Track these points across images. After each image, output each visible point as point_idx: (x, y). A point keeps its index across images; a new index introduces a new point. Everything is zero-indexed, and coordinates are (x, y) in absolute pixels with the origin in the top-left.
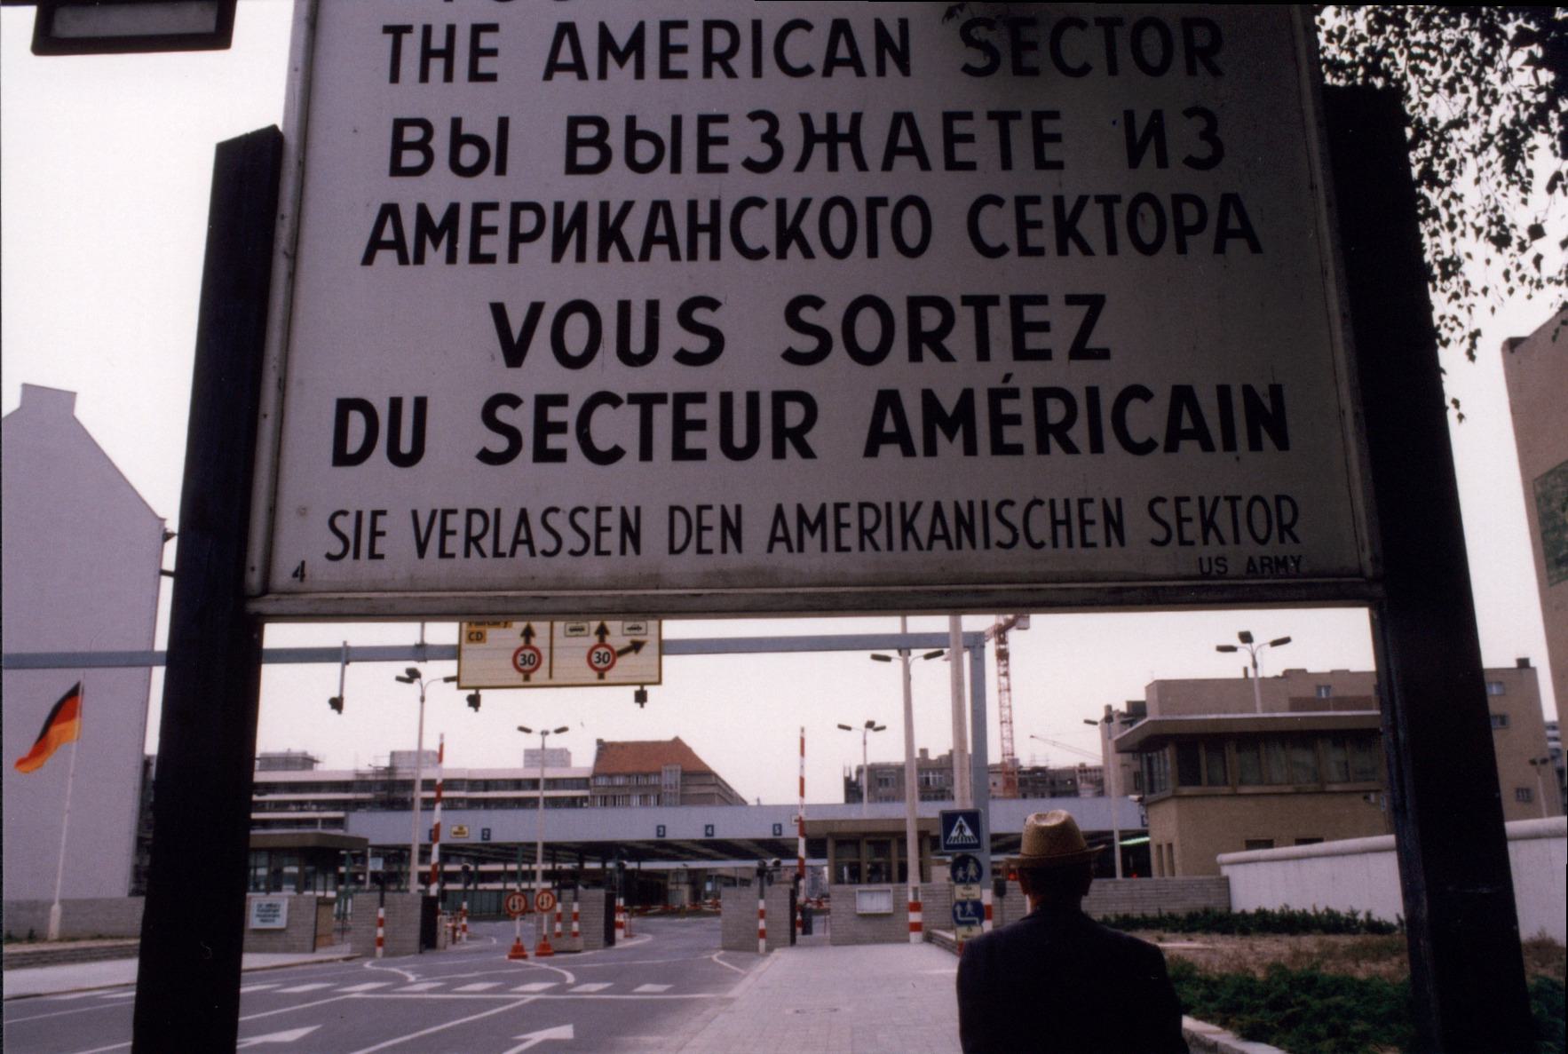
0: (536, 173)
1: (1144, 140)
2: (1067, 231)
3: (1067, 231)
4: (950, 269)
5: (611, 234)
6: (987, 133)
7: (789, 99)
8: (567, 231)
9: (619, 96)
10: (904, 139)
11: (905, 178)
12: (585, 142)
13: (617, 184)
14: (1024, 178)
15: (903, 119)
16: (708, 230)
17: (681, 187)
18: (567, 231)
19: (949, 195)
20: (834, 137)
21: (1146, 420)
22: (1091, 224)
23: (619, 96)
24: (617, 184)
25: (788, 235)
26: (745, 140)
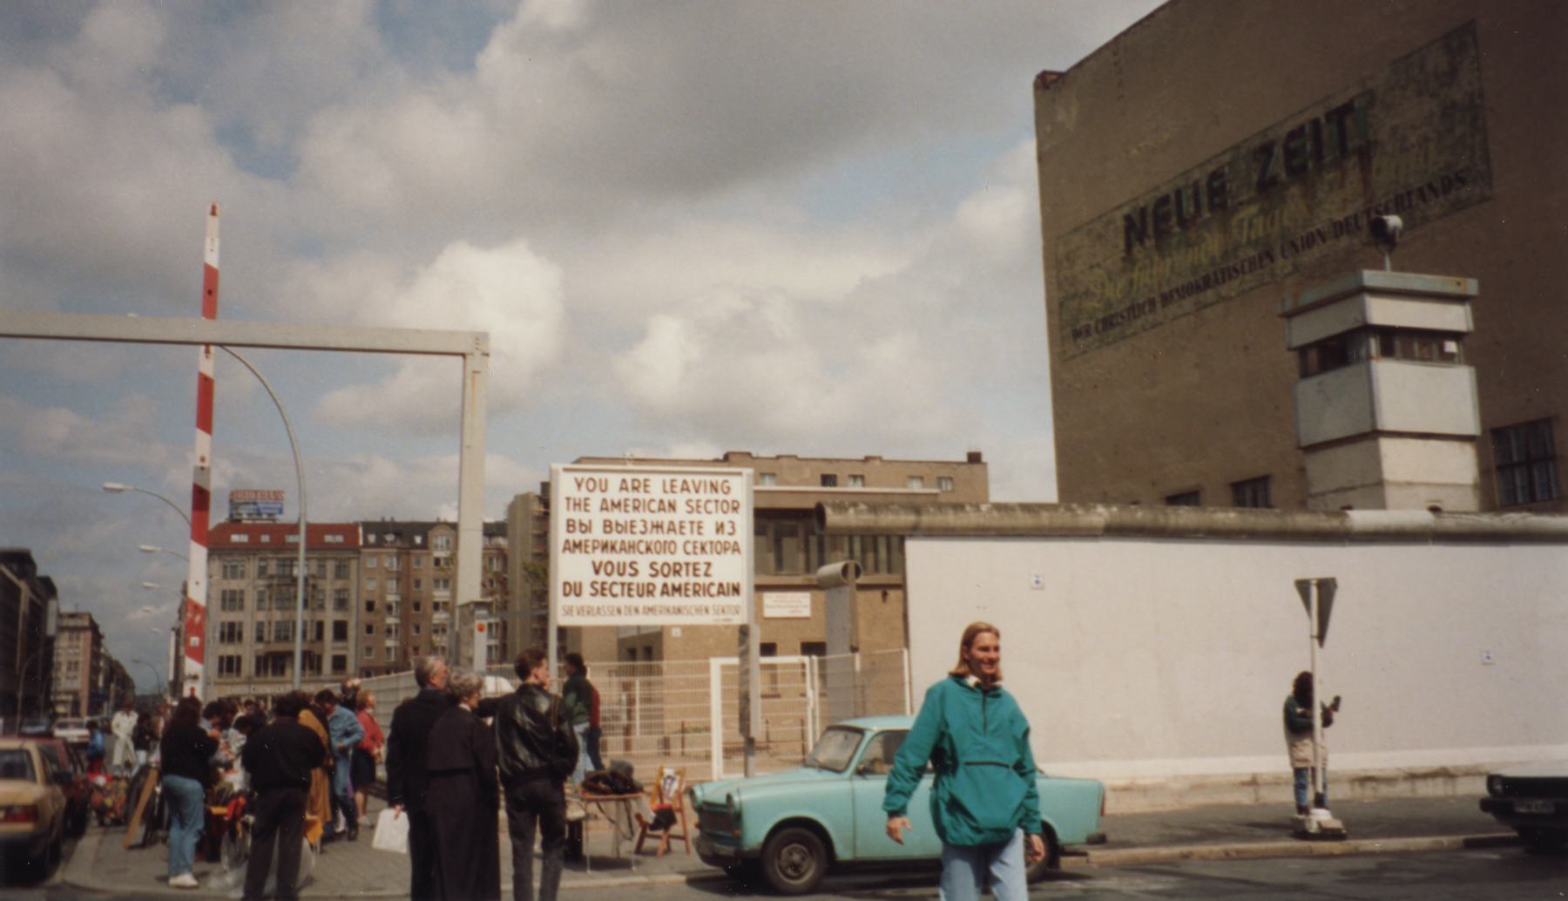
0: (598, 533)
1: (720, 528)
2: (703, 548)
3: (703, 548)
4: (680, 557)
5: (613, 548)
6: (687, 526)
7: (651, 518)
8: (605, 547)
9: (616, 516)
10: (672, 529)
11: (671, 537)
12: (607, 526)
13: (614, 537)
14: (696, 537)
15: (672, 523)
16: (632, 547)
17: (627, 537)
18: (605, 547)
19: (680, 540)
20: (658, 526)
21: (714, 590)
22: (708, 548)
23: (616, 516)
24: (614, 537)
25: (648, 549)
26: (639, 527)
